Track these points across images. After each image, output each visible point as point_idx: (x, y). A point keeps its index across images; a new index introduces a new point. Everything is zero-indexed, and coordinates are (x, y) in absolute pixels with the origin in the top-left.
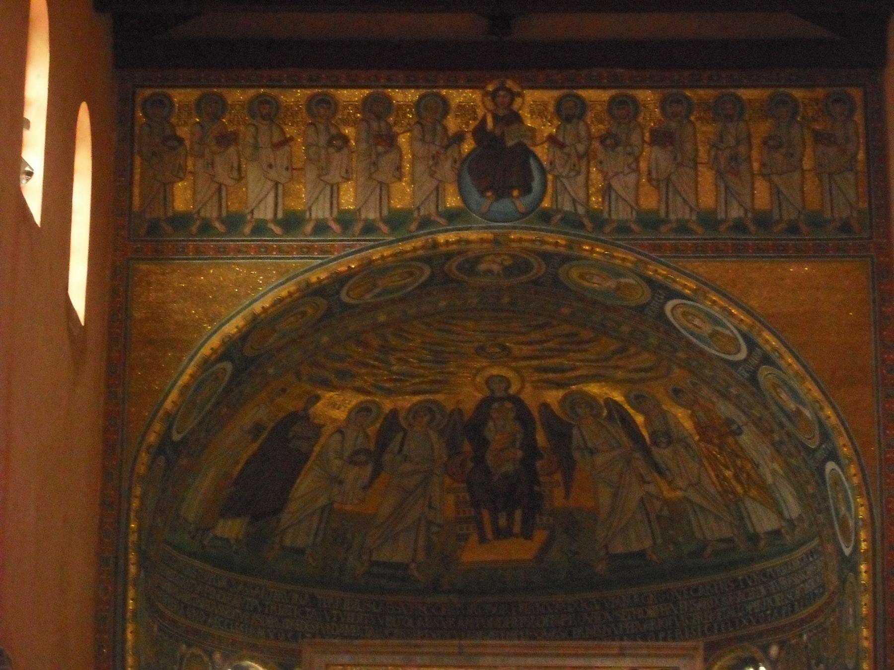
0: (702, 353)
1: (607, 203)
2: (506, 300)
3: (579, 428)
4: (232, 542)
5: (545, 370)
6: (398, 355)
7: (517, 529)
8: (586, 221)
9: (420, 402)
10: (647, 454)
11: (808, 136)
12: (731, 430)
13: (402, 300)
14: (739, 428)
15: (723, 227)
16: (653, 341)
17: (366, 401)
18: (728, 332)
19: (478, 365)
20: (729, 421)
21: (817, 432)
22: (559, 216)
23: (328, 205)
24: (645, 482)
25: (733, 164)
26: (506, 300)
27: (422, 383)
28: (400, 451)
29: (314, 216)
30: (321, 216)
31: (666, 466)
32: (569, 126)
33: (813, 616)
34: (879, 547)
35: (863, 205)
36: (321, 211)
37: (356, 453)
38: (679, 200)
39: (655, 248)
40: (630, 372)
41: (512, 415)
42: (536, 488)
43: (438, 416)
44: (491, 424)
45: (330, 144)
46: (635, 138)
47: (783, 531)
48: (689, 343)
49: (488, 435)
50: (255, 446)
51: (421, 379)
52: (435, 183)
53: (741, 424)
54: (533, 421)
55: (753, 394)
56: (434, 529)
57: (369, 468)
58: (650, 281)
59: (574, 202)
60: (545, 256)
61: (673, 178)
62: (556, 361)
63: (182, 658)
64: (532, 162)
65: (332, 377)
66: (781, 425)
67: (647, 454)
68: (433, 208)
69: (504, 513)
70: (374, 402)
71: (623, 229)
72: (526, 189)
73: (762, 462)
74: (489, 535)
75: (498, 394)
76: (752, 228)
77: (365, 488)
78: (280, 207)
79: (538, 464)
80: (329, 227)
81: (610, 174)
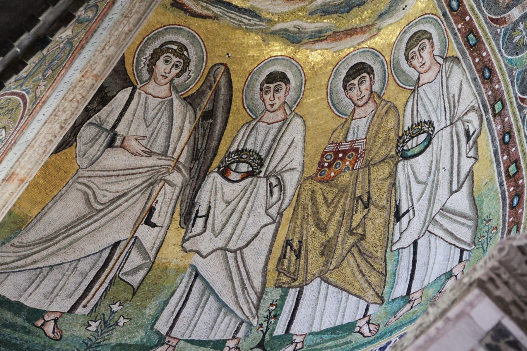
31: (209, 208)
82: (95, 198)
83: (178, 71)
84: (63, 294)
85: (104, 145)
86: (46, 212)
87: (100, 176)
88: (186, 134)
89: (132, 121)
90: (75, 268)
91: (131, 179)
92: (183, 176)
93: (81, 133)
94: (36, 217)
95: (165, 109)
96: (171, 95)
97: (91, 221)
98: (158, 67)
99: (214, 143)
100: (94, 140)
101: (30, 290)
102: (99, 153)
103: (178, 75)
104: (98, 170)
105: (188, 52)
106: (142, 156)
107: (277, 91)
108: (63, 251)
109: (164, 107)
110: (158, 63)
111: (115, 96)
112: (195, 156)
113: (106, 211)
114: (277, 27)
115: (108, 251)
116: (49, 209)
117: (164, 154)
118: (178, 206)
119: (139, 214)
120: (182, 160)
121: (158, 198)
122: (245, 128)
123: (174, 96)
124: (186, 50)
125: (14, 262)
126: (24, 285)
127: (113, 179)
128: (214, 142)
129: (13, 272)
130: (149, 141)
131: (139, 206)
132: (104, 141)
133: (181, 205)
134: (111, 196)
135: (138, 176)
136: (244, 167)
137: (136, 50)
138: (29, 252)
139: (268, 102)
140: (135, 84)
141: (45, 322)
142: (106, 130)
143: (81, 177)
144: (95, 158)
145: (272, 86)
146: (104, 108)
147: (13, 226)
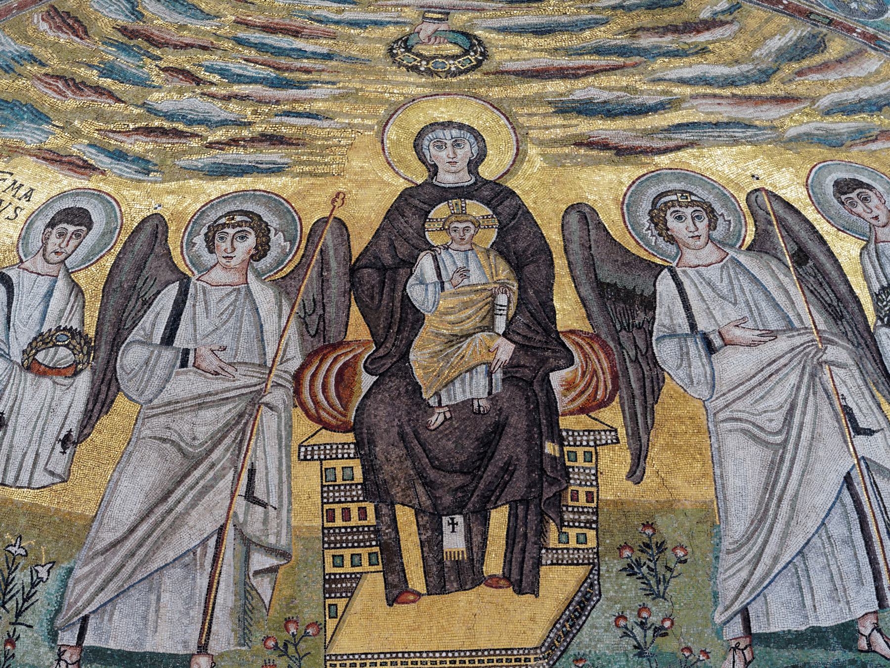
3: (675, 277)
5: (586, 109)
6: (172, 59)
7: (494, 564)
9: (223, 199)
17: (77, 193)
19: (396, 94)
24: (859, 431)
27: (234, 142)
28: (168, 339)
37: (42, 341)
40: (828, 112)
42: (550, 448)
43: (277, 240)
44: (426, 263)
49: (415, 293)
51: (233, 132)
56: (260, 561)
57: (84, 381)
62: (613, 80)
69: (459, 519)
70: (99, 195)
74: (417, 580)
75: (446, 178)
77: (66, 442)
79: (556, 379)
82: (762, 429)
83: (706, 221)
84: (851, 586)
85: (703, 353)
86: (723, 484)
87: (739, 398)
88: (796, 292)
89: (709, 308)
90: (829, 538)
91: (780, 379)
92: (843, 347)
93: (660, 358)
94: (717, 497)
95: (736, 273)
96: (728, 254)
97: (787, 464)
98: (675, 230)
99: (843, 288)
100: (684, 355)
101: (808, 602)
102: (708, 368)
103: (712, 226)
104: (729, 391)
105: (696, 195)
106: (765, 342)
107: (865, 200)
108: (793, 523)
109: (732, 273)
110: (669, 225)
111: (655, 290)
112: (835, 315)
113: (792, 440)
114: (792, 132)
115: (846, 492)
116: (722, 477)
117: (790, 327)
118: (878, 394)
119: (836, 424)
120: (822, 327)
121: (840, 392)
122: (866, 256)
123: (732, 253)
124: (691, 194)
125: (752, 574)
126: (795, 597)
127: (759, 393)
128: (841, 287)
129: (765, 588)
130: (755, 321)
131: (826, 413)
132: (698, 348)
133: (878, 390)
134: (779, 416)
135: (785, 371)
137: (627, 227)
138: (756, 549)
139: (868, 217)
140: (666, 264)
141: (868, 638)
142: (687, 334)
143: (718, 412)
144: (709, 378)
145: (853, 195)
146: (657, 311)
147: (706, 527)
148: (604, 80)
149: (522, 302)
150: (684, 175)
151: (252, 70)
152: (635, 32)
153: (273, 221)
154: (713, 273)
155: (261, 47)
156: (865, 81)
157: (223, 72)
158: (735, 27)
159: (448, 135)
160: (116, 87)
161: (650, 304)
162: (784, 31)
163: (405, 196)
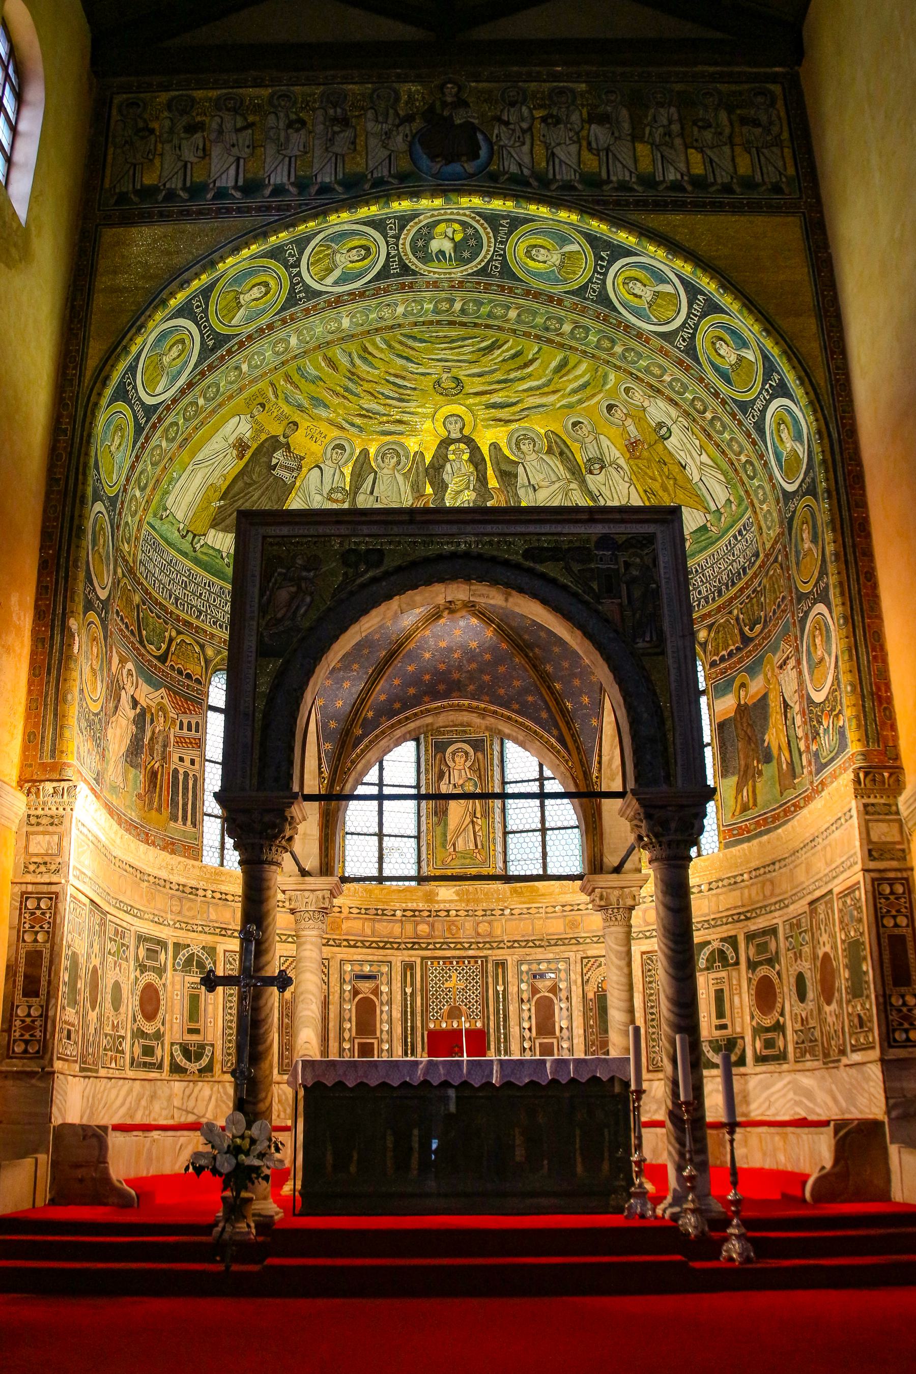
0: (639, 335)
1: (551, 168)
2: (458, 306)
4: (224, 555)
5: (494, 406)
6: (366, 386)
8: (531, 180)
10: (583, 482)
11: (733, 117)
12: (661, 432)
13: (362, 295)
14: (669, 429)
15: (661, 187)
16: (593, 338)
18: (668, 289)
20: (660, 425)
21: (761, 371)
22: (506, 176)
23: (285, 173)
25: (667, 138)
26: (458, 306)
27: (388, 422)
28: (372, 493)
29: (272, 181)
30: (279, 181)
32: (512, 110)
33: (742, 590)
34: (838, 457)
35: (791, 171)
36: (279, 177)
37: (332, 491)
38: (619, 165)
39: (598, 202)
41: (466, 457)
43: (403, 459)
44: (448, 466)
45: (290, 125)
46: (575, 117)
47: (709, 525)
48: (628, 327)
49: (445, 477)
50: (242, 463)
52: (387, 153)
53: (669, 423)
54: (484, 459)
55: (688, 368)
58: (593, 240)
59: (520, 165)
60: (492, 219)
61: (612, 148)
63: (171, 640)
64: (480, 137)
65: (306, 403)
66: (716, 395)
67: (583, 482)
68: (386, 173)
71: (568, 187)
72: (475, 156)
73: (689, 461)
75: (455, 435)
76: (689, 188)
78: (241, 176)
80: (288, 190)
81: (553, 144)
100: (527, 493)
112: (573, 474)
136: (597, 466)
148: (501, 394)
149: (478, 479)
150: (525, 429)
151: (392, 394)
152: (508, 372)
153: (402, 453)
154: (534, 463)
155: (394, 384)
156: (581, 376)
157: (383, 394)
158: (539, 361)
159: (453, 419)
160: (350, 397)
161: (516, 476)
162: (555, 356)
163: (442, 442)
